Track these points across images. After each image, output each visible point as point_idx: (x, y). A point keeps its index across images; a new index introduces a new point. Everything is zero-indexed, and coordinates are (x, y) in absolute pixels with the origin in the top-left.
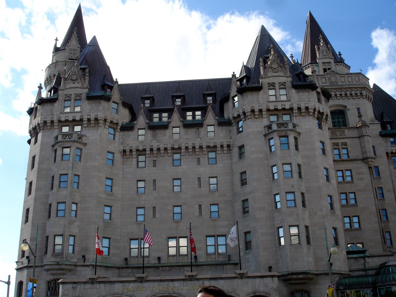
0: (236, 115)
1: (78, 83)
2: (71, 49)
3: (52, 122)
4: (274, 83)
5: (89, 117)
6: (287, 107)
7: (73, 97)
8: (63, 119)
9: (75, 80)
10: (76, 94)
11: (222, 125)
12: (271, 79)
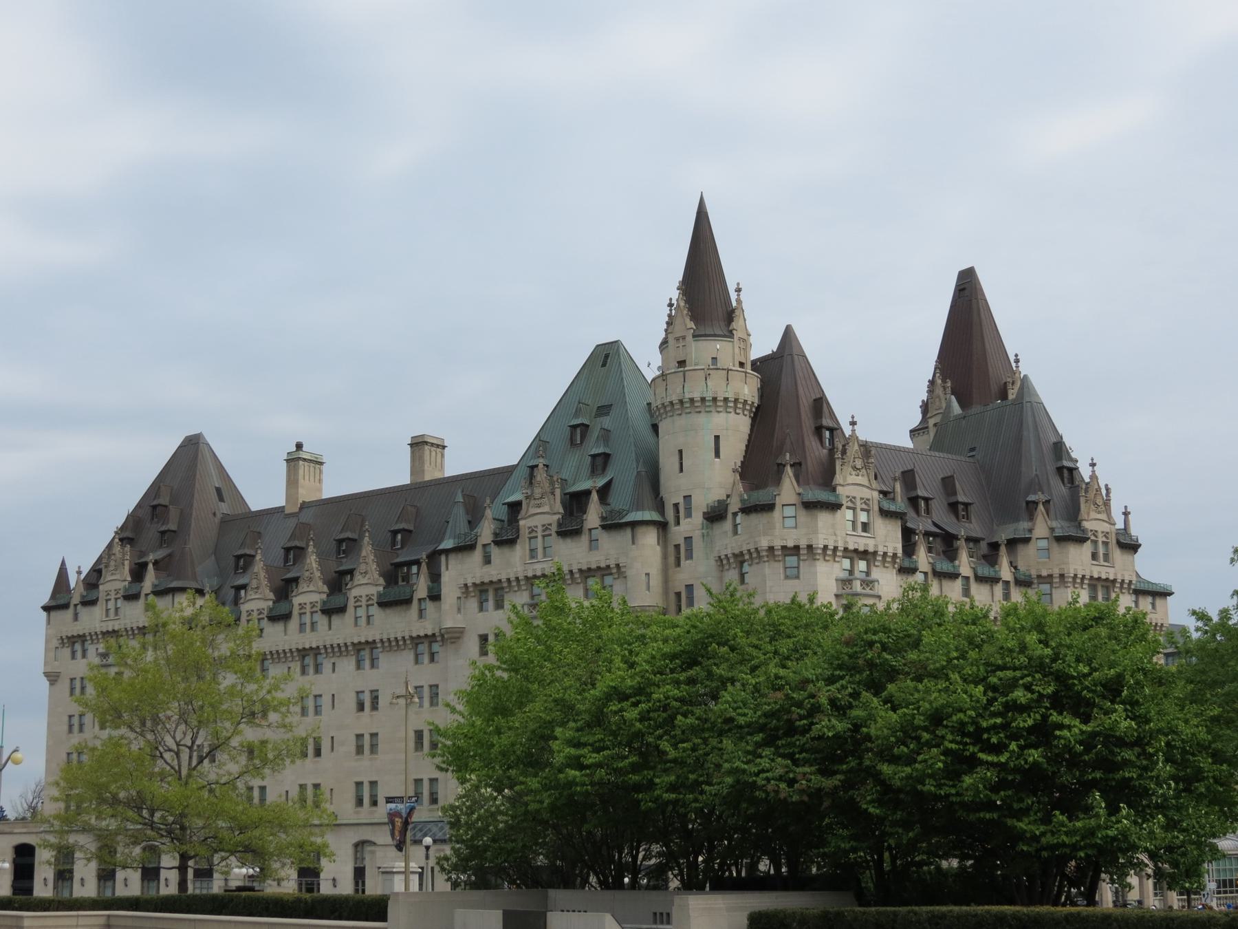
0: (1044, 573)
1: (863, 475)
2: (740, 339)
3: (836, 549)
4: (1096, 531)
5: (885, 549)
6: (1111, 578)
7: (859, 505)
8: (851, 547)
9: (858, 469)
10: (862, 499)
11: (1020, 585)
12: (1094, 522)
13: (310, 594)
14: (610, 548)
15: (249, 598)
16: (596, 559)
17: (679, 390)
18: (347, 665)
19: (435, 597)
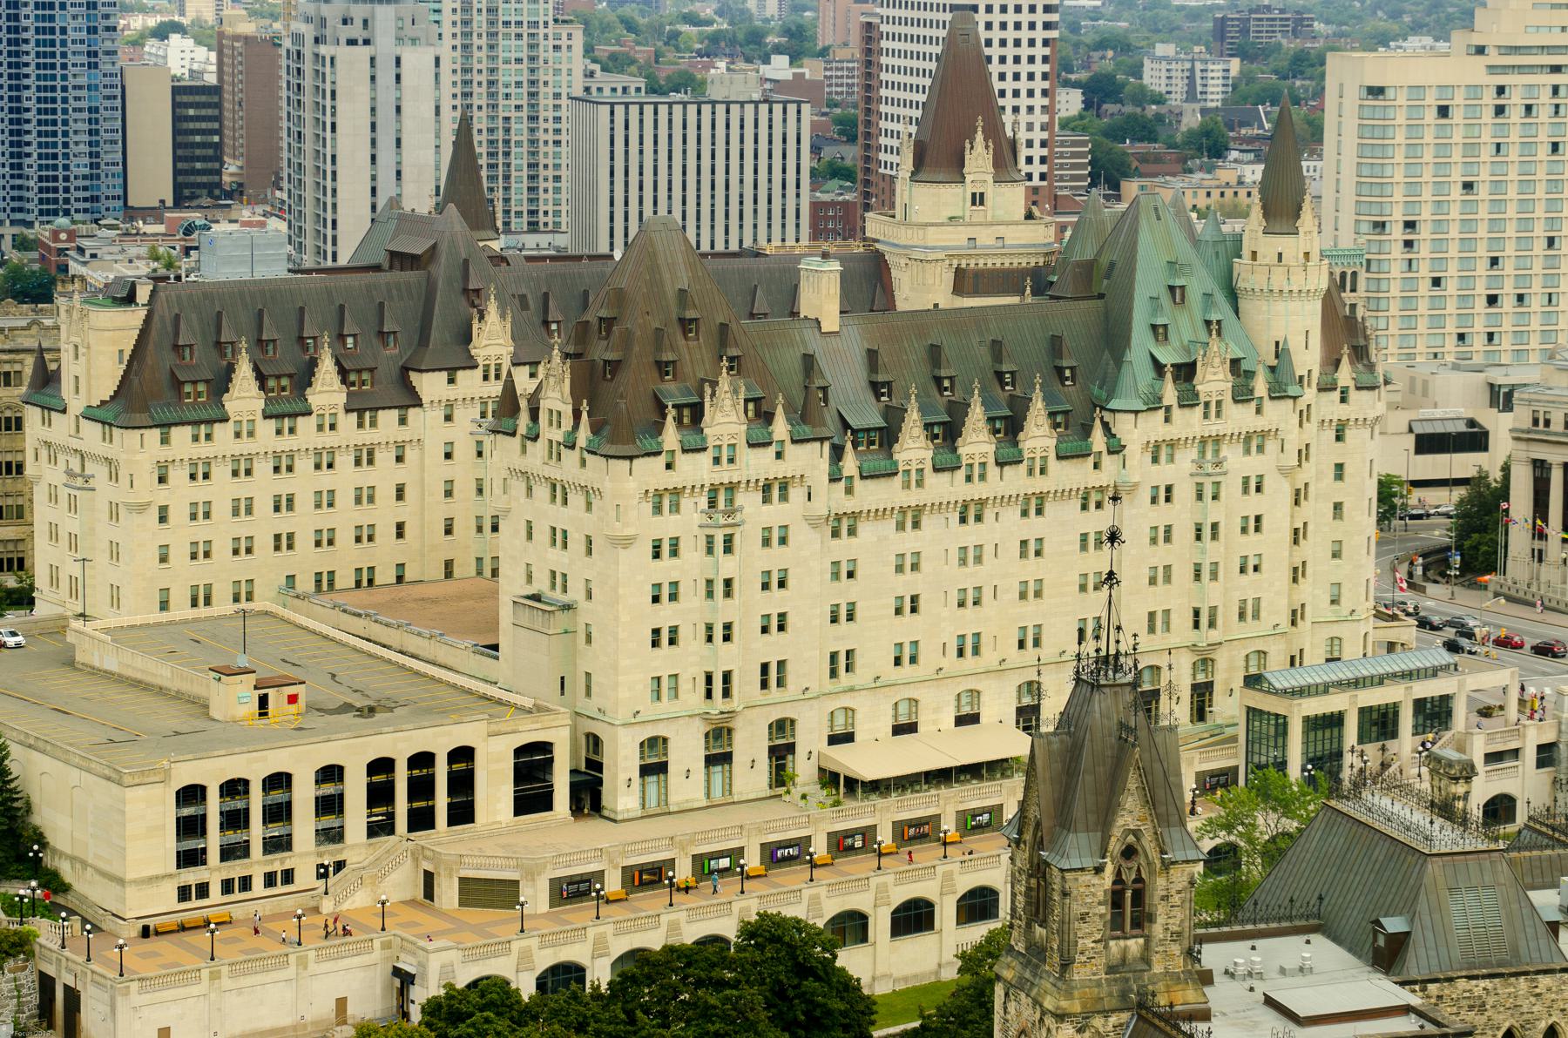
13: (977, 442)
14: (1278, 415)
15: (906, 446)
16: (1260, 423)
17: (1316, 281)
18: (1012, 513)
19: (1116, 449)
